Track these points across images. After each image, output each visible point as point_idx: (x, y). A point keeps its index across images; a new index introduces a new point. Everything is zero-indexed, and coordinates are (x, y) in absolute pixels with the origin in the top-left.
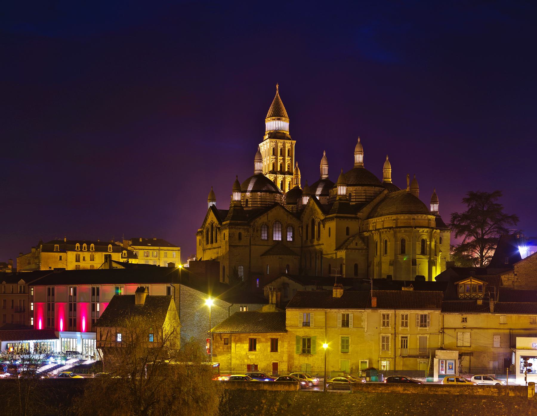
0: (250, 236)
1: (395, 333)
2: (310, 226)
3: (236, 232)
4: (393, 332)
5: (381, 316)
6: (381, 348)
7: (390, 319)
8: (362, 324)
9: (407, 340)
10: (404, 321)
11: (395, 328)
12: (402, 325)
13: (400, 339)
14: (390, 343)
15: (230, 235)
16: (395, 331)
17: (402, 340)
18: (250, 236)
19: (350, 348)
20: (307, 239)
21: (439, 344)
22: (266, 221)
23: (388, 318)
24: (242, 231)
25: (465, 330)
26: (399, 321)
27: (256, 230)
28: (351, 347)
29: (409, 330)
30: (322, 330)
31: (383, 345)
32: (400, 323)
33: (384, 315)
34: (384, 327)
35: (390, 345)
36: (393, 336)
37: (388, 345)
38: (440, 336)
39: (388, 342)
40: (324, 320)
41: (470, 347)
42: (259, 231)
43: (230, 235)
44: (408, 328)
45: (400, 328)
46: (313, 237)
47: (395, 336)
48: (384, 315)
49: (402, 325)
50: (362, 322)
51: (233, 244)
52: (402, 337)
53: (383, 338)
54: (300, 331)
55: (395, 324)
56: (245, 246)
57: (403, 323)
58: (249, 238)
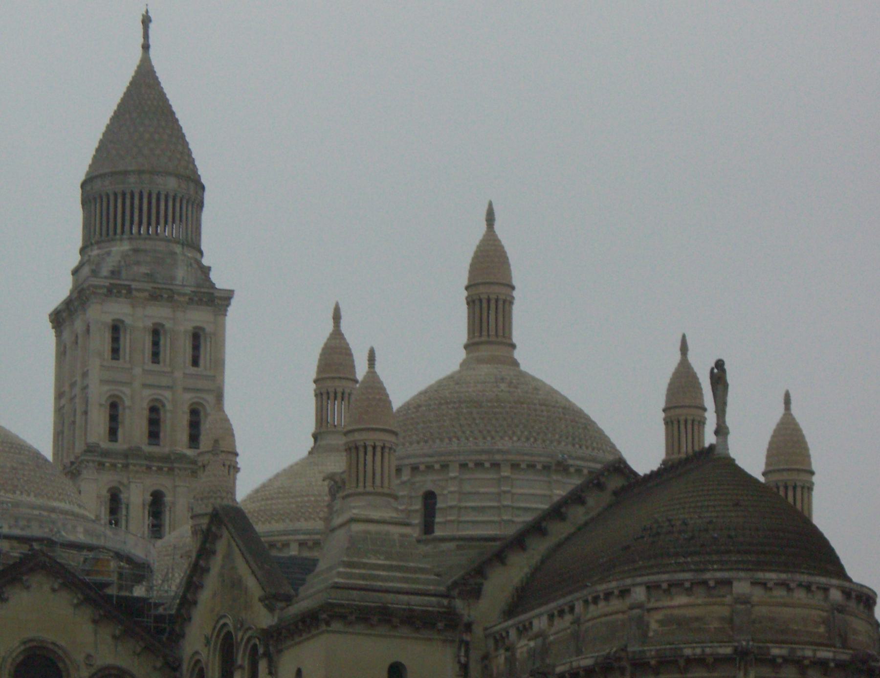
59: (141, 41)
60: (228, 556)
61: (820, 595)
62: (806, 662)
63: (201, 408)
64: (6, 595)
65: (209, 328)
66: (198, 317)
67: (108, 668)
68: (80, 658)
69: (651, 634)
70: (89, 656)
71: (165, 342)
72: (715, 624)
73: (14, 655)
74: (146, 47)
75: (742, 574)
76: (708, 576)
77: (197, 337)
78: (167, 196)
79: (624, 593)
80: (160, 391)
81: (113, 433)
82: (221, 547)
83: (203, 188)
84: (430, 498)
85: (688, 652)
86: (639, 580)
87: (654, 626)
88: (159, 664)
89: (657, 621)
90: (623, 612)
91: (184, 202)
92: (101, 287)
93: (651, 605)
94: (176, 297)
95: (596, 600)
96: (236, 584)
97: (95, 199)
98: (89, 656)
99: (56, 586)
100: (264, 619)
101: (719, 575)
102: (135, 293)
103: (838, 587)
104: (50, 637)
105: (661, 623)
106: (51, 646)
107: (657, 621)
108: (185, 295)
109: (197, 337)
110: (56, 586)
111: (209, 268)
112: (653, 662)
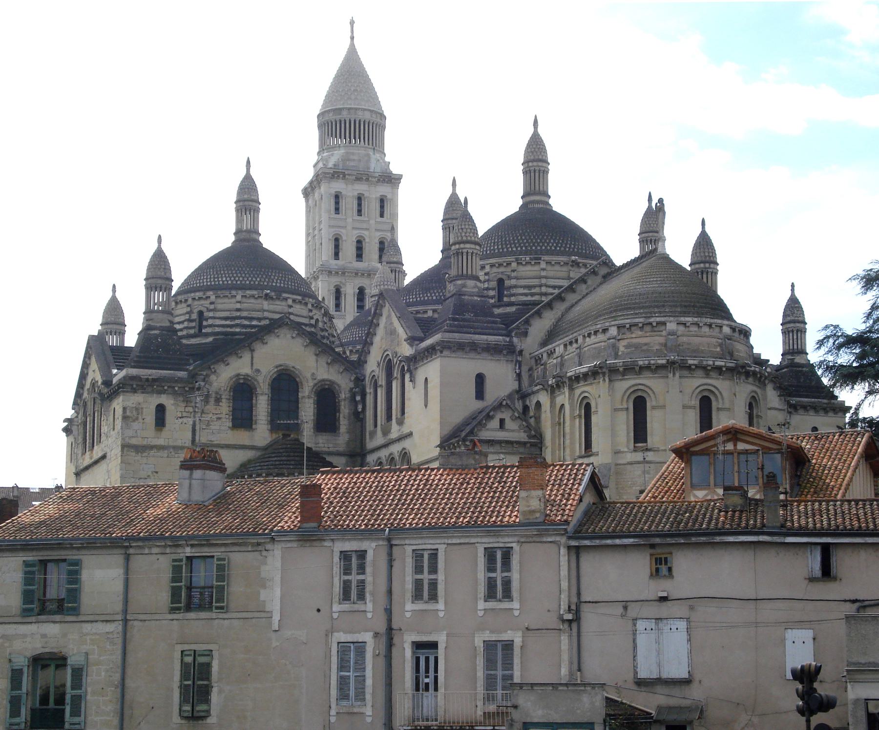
1: (390, 629)
2: (382, 381)
3: (149, 402)
4: (382, 628)
5: (336, 559)
6: (334, 692)
7: (369, 570)
8: (263, 595)
9: (436, 659)
10: (426, 577)
11: (389, 612)
12: (417, 595)
13: (408, 653)
14: (369, 673)
15: (128, 413)
16: (390, 620)
17: (418, 660)
19: (214, 697)
20: (376, 426)
21: (564, 671)
22: (246, 370)
23: (362, 569)
25: (665, 610)
26: (405, 577)
27: (212, 400)
28: (220, 692)
29: (441, 614)
30: (110, 627)
31: (343, 683)
32: (409, 586)
33: (345, 556)
34: (346, 606)
35: (369, 682)
36: (383, 640)
37: (361, 680)
38: (564, 639)
39: (364, 669)
40: (119, 587)
41: (687, 682)
42: (224, 400)
43: (128, 413)
44: (441, 606)
45: (409, 606)
46: (389, 417)
47: (390, 645)
48: (345, 556)
49: (417, 595)
50: (264, 586)
51: (134, 441)
52: (419, 646)
53: (344, 648)
54: (25, 636)
55: (390, 592)
56: (175, 448)
57: (418, 584)
59: (350, 34)
60: (389, 316)
61: (717, 329)
62: (709, 368)
64: (266, 341)
65: (389, 196)
66: (383, 190)
67: (323, 380)
68: (309, 375)
69: (620, 353)
70: (313, 374)
71: (365, 204)
72: (658, 347)
73: (271, 374)
74: (352, 38)
75: (672, 319)
76: (652, 320)
77: (382, 201)
79: (605, 331)
80: (363, 232)
82: (385, 311)
83: (385, 118)
84: (501, 282)
85: (641, 363)
86: (613, 323)
87: (622, 349)
88: (353, 378)
89: (624, 346)
90: (605, 342)
91: (375, 126)
92: (328, 173)
93: (619, 338)
94: (370, 179)
95: (589, 335)
96: (392, 332)
98: (313, 374)
99: (294, 335)
100: (407, 350)
101: (658, 319)
102: (347, 177)
103: (727, 325)
104: (290, 363)
105: (626, 347)
106: (292, 369)
107: (624, 346)
109: (382, 201)
110: (294, 335)
112: (621, 369)
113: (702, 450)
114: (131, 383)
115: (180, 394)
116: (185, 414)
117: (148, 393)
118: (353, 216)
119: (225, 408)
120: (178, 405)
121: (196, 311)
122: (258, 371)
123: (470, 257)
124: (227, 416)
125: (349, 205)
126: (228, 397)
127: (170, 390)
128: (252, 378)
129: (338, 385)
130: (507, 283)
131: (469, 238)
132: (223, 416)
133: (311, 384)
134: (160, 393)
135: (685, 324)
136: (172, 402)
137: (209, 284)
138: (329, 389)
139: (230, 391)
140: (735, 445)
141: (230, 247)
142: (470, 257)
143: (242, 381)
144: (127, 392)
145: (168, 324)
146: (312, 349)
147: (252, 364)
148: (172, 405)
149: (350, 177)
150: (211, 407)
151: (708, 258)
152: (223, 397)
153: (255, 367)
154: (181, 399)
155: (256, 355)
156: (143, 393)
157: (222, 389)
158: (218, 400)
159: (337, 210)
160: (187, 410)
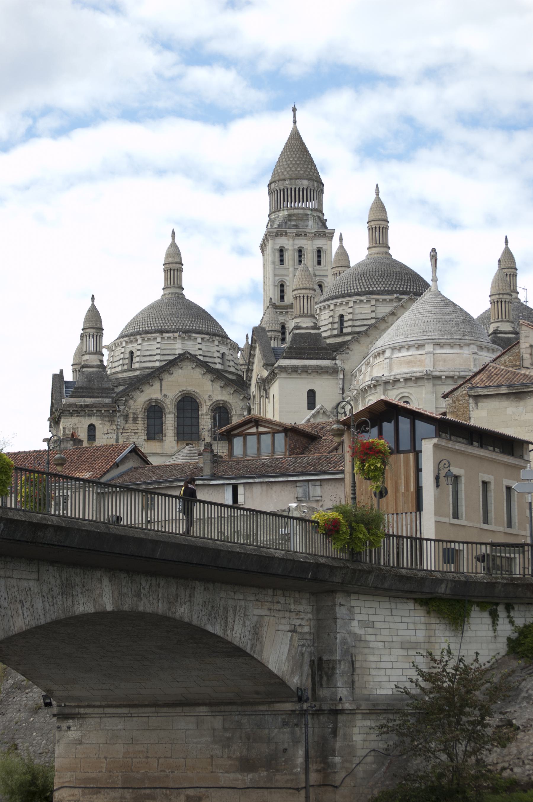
0: (118, 433)
18: (118, 433)
24: (94, 420)
27: (131, 419)
42: (139, 419)
58: (115, 437)
59: (292, 119)
62: (456, 377)
63: (322, 284)
64: (171, 372)
65: (324, 247)
66: (320, 242)
68: (206, 397)
70: (210, 396)
73: (177, 397)
74: (295, 122)
77: (319, 252)
78: (303, 189)
81: (282, 298)
83: (323, 185)
91: (312, 191)
92: (273, 233)
94: (308, 234)
97: (274, 192)
99: (194, 366)
104: (191, 389)
108: (312, 233)
109: (319, 252)
110: (194, 366)
111: (326, 220)
112: (391, 381)
113: (238, 433)
114: (68, 409)
115: (105, 416)
116: (110, 431)
117: (82, 416)
118: (295, 265)
119: (141, 425)
120: (105, 424)
121: (128, 351)
122: (165, 396)
123: (305, 300)
124: (143, 431)
125: (290, 256)
126: (143, 416)
127: (98, 413)
128: (161, 401)
129: (229, 403)
130: (346, 318)
131: (305, 285)
132: (139, 431)
133: (209, 404)
134: (90, 415)
135: (460, 345)
136: (100, 422)
137: (138, 330)
138: (223, 407)
139: (144, 412)
140: (257, 428)
141: (159, 300)
142: (305, 300)
143: (154, 404)
144: (66, 415)
145: (99, 363)
146: (209, 377)
147: (161, 390)
148: (100, 424)
149: (290, 235)
150: (130, 424)
151: (502, 290)
152: (139, 416)
153: (163, 393)
154: (107, 419)
155: (164, 383)
156: (78, 416)
157: (138, 411)
158: (135, 419)
159: (282, 261)
160: (111, 428)
